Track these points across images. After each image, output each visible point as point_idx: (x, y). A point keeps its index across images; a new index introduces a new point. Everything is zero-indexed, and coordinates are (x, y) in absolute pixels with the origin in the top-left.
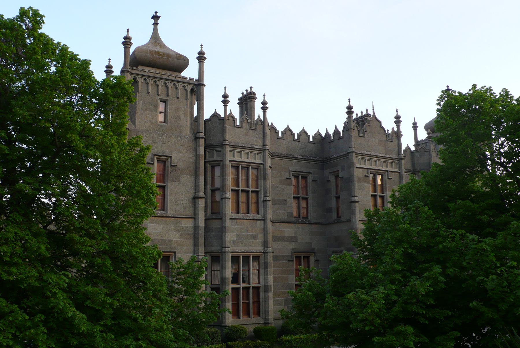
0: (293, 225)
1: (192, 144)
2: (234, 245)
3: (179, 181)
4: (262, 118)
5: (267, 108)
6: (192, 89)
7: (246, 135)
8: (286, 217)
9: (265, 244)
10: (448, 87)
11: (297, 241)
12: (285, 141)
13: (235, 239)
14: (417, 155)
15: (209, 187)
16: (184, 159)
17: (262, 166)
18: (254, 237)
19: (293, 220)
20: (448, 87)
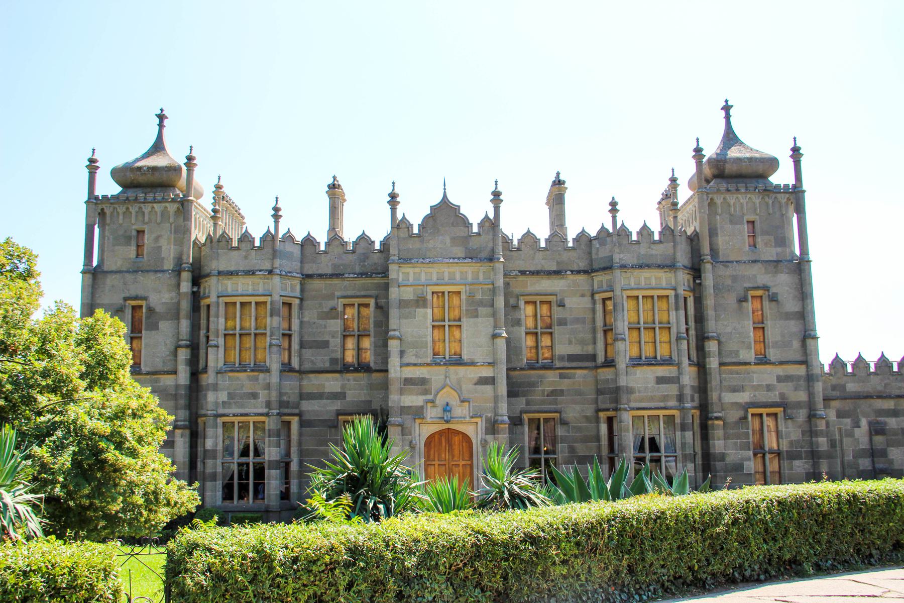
0: (337, 375)
1: (173, 281)
2: (224, 407)
3: (157, 329)
4: (273, 232)
5: (281, 216)
6: (178, 208)
7: (246, 257)
8: (327, 365)
9: (268, 404)
10: (726, 101)
11: (345, 397)
12: (329, 255)
13: (226, 399)
14: (596, 244)
15: (203, 332)
16: (164, 300)
17: (269, 298)
18: (254, 396)
19: (339, 368)
20: (726, 101)
